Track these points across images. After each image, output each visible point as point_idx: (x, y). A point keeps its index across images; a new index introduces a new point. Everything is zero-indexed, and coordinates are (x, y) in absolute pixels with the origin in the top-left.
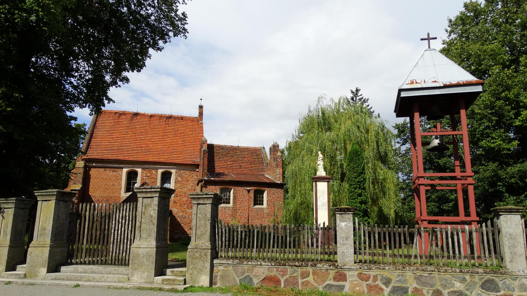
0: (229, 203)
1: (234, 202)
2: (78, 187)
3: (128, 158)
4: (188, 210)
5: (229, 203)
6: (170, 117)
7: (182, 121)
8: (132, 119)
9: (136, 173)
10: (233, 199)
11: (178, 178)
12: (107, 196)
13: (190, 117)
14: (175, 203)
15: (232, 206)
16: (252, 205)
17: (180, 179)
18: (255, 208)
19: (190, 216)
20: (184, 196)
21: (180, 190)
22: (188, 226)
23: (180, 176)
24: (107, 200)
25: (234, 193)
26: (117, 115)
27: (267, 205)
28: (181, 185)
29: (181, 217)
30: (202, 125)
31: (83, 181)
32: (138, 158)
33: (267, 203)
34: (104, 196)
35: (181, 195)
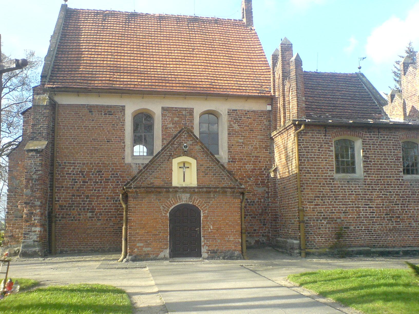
1: (367, 169)
3: (133, 86)
6: (195, 20)
7: (216, 25)
8: (128, 23)
11: (233, 125)
12: (99, 163)
13: (228, 19)
15: (363, 177)
17: (236, 127)
18: (408, 180)
19: (262, 200)
20: (248, 162)
21: (238, 149)
22: (260, 220)
24: (97, 172)
26: (100, 17)
30: (253, 32)
32: (153, 87)
35: (242, 159)
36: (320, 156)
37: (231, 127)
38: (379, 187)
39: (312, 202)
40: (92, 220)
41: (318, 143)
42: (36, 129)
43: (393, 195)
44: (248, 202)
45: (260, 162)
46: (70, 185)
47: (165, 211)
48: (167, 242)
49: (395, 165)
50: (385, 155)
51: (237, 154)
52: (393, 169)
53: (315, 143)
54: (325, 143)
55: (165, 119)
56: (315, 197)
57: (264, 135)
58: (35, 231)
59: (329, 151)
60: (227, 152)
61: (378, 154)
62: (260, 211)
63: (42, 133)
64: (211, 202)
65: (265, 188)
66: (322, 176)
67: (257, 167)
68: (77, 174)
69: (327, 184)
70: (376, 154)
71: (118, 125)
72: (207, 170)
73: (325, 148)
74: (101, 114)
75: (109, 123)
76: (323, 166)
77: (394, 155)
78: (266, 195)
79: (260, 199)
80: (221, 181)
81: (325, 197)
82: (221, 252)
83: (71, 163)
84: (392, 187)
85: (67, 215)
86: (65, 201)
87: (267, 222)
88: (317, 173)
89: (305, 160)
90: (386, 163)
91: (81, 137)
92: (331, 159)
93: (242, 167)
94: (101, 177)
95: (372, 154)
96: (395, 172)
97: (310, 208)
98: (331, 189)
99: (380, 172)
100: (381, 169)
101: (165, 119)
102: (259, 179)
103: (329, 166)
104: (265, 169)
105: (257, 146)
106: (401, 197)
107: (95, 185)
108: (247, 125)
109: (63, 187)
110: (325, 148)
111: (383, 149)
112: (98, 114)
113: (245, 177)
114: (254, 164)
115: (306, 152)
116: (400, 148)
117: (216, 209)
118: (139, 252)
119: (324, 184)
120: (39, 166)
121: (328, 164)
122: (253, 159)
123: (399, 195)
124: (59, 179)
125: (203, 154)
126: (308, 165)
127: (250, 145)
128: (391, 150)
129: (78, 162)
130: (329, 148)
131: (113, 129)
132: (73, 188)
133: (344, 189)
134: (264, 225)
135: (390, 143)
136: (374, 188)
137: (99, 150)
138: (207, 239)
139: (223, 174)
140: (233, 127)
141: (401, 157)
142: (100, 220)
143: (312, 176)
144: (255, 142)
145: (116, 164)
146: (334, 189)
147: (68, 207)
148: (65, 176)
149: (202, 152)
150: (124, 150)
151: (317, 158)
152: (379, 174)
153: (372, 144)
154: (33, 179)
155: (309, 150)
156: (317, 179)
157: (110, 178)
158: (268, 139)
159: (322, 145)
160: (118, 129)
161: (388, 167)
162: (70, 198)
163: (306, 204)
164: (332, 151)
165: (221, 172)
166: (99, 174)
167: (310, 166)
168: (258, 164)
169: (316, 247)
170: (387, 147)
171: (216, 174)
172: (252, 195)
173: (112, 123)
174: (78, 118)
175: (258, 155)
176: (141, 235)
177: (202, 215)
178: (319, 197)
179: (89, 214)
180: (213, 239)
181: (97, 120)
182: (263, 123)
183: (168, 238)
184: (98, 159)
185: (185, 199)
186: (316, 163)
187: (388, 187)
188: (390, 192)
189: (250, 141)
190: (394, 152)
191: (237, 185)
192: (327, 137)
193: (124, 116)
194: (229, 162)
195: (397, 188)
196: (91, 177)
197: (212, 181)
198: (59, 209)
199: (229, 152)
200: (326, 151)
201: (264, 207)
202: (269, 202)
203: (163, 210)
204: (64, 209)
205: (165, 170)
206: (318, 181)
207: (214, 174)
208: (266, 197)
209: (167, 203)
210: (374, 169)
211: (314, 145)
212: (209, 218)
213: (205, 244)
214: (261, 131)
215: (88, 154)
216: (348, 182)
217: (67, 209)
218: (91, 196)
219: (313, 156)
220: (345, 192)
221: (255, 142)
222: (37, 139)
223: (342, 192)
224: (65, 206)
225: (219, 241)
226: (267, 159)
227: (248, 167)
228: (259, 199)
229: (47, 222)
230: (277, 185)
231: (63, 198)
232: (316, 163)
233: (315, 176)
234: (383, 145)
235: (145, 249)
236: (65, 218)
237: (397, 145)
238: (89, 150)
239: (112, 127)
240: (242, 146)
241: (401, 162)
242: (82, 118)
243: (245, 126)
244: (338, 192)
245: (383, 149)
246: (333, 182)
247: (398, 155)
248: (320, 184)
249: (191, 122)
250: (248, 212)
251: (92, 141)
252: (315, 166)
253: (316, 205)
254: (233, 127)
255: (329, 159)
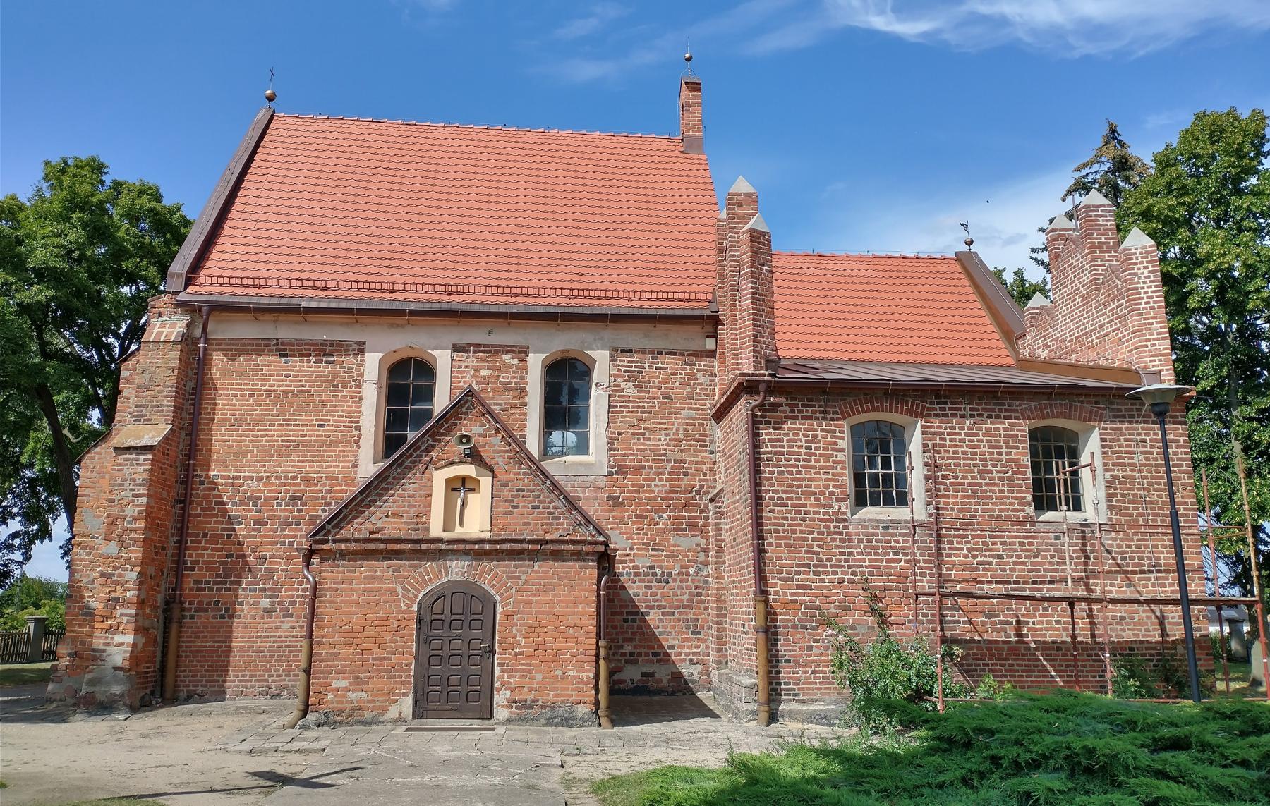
0: (903, 500)
1: (934, 495)
2: (154, 433)
4: (680, 540)
5: (903, 500)
9: (425, 370)
10: (927, 477)
11: (623, 385)
12: (295, 478)
14: (615, 505)
16: (1031, 510)
17: (629, 390)
19: (692, 571)
21: (633, 442)
22: (687, 620)
23: (630, 375)
24: (292, 498)
25: (925, 445)
27: (1110, 507)
28: (640, 420)
29: (646, 574)
31: (177, 408)
33: (1110, 497)
34: (277, 478)
36: (813, 463)
37: (617, 391)
38: (967, 543)
39: (791, 579)
40: (271, 617)
41: (805, 429)
42: (146, 397)
43: (1007, 564)
44: (655, 574)
45: (686, 474)
46: (223, 530)
47: (409, 599)
48: (409, 676)
49: (1009, 486)
50: (985, 460)
51: (631, 455)
52: (1007, 498)
53: (800, 429)
54: (822, 431)
55: (459, 372)
56: (798, 566)
57: (698, 409)
58: (121, 644)
59: (833, 450)
60: (607, 448)
61: (964, 459)
62: (686, 597)
63: (162, 405)
64: (524, 577)
65: (698, 539)
66: (818, 513)
67: (679, 486)
68: (242, 504)
69: (829, 534)
70: (959, 458)
71: (345, 387)
72: (517, 496)
73: (825, 442)
74: (309, 361)
75: (325, 382)
76: (819, 486)
77: (1007, 460)
78: (702, 557)
79: (687, 567)
80: (551, 524)
81: (826, 566)
82: (543, 707)
83: (229, 477)
84: (1004, 543)
85: (209, 603)
86: (208, 569)
87: (702, 627)
88: (805, 506)
89: (772, 473)
90: (988, 481)
91: (256, 415)
92: (839, 471)
93: (643, 486)
94: (300, 511)
95: (949, 458)
96: (1011, 504)
97: (785, 594)
98: (842, 547)
99: (968, 503)
100: (973, 497)
101: (459, 372)
102: (684, 517)
103: (834, 486)
104: (698, 493)
105: (681, 436)
106: (1029, 570)
107: (283, 530)
108: (657, 384)
109: (205, 535)
110: (825, 442)
111: (979, 447)
112: (301, 361)
113: (648, 511)
114: (672, 480)
115: (776, 453)
116: (1023, 442)
117: (535, 596)
118: (339, 702)
119: (822, 533)
120: (140, 485)
121: (831, 484)
122: (669, 468)
123: (1024, 564)
124: (199, 516)
125: (509, 458)
126: (779, 485)
127: (663, 432)
128: (1001, 447)
129: (247, 474)
130: (836, 443)
131: (334, 397)
132: (229, 536)
133: (874, 548)
134: (694, 633)
135: (998, 429)
136: (955, 545)
137: (298, 446)
138: (512, 671)
139: (555, 508)
140: (623, 391)
141: (1026, 466)
142: (291, 616)
143: (790, 512)
144: (676, 426)
145: (337, 479)
146: (848, 547)
147: (215, 583)
148: (213, 509)
149: (506, 452)
150: (358, 447)
151: (803, 466)
152: (969, 510)
153: (949, 434)
154: (123, 518)
155: (782, 447)
156: (804, 519)
157: (320, 513)
158: (706, 419)
159: (815, 436)
160: (345, 397)
161: (993, 491)
162: (221, 563)
163: (775, 585)
164: (842, 450)
165: (552, 502)
166: (295, 505)
167: (785, 488)
168: (682, 480)
169: (801, 697)
170: (987, 441)
171: (538, 507)
172: (666, 556)
173: (332, 381)
174: (253, 370)
175: (683, 456)
176: (344, 659)
177: (499, 609)
178: (809, 566)
179: (265, 603)
180: (524, 671)
181: (298, 376)
182: (696, 379)
183: (413, 667)
184: (293, 466)
185: (457, 569)
186: (799, 479)
187: (993, 544)
188: (1000, 557)
189: (665, 423)
190: (1007, 454)
191: (591, 535)
192: (828, 416)
193: (362, 365)
194: (610, 474)
195: (1017, 546)
196: (276, 511)
197: (529, 524)
198: (191, 589)
199: (610, 450)
200: (825, 449)
201: (696, 588)
202: (708, 576)
203: (404, 596)
204: (204, 589)
205: (414, 496)
206: (807, 526)
207: (534, 508)
208: (701, 563)
209: (414, 578)
210: (956, 497)
211: (797, 435)
212: (516, 617)
213: (503, 684)
214: (690, 398)
215: (273, 456)
216: (885, 528)
217: (211, 589)
218: (273, 556)
219: (793, 462)
220: (876, 554)
221: (676, 426)
222: (148, 420)
223: (869, 554)
224: (208, 582)
225: (539, 677)
226: (705, 467)
227: (656, 486)
228: (682, 567)
229: (161, 621)
230: (723, 532)
231: (204, 562)
232: (799, 479)
233: (799, 512)
234: (977, 435)
235: (352, 695)
236: (206, 610)
237: (1016, 436)
238: (274, 446)
239: (331, 392)
240: (644, 434)
241: (1028, 479)
242: (261, 370)
243: (651, 387)
244: (858, 554)
245: (979, 447)
246: (846, 527)
247: (1018, 460)
248: (811, 533)
249: (522, 378)
250: (654, 601)
251: (281, 425)
252: (799, 486)
253: (798, 587)
254: (623, 391)
255: (835, 471)
